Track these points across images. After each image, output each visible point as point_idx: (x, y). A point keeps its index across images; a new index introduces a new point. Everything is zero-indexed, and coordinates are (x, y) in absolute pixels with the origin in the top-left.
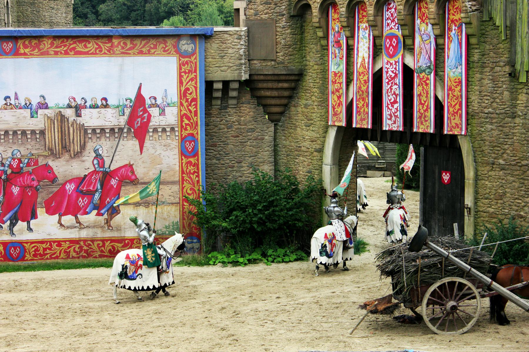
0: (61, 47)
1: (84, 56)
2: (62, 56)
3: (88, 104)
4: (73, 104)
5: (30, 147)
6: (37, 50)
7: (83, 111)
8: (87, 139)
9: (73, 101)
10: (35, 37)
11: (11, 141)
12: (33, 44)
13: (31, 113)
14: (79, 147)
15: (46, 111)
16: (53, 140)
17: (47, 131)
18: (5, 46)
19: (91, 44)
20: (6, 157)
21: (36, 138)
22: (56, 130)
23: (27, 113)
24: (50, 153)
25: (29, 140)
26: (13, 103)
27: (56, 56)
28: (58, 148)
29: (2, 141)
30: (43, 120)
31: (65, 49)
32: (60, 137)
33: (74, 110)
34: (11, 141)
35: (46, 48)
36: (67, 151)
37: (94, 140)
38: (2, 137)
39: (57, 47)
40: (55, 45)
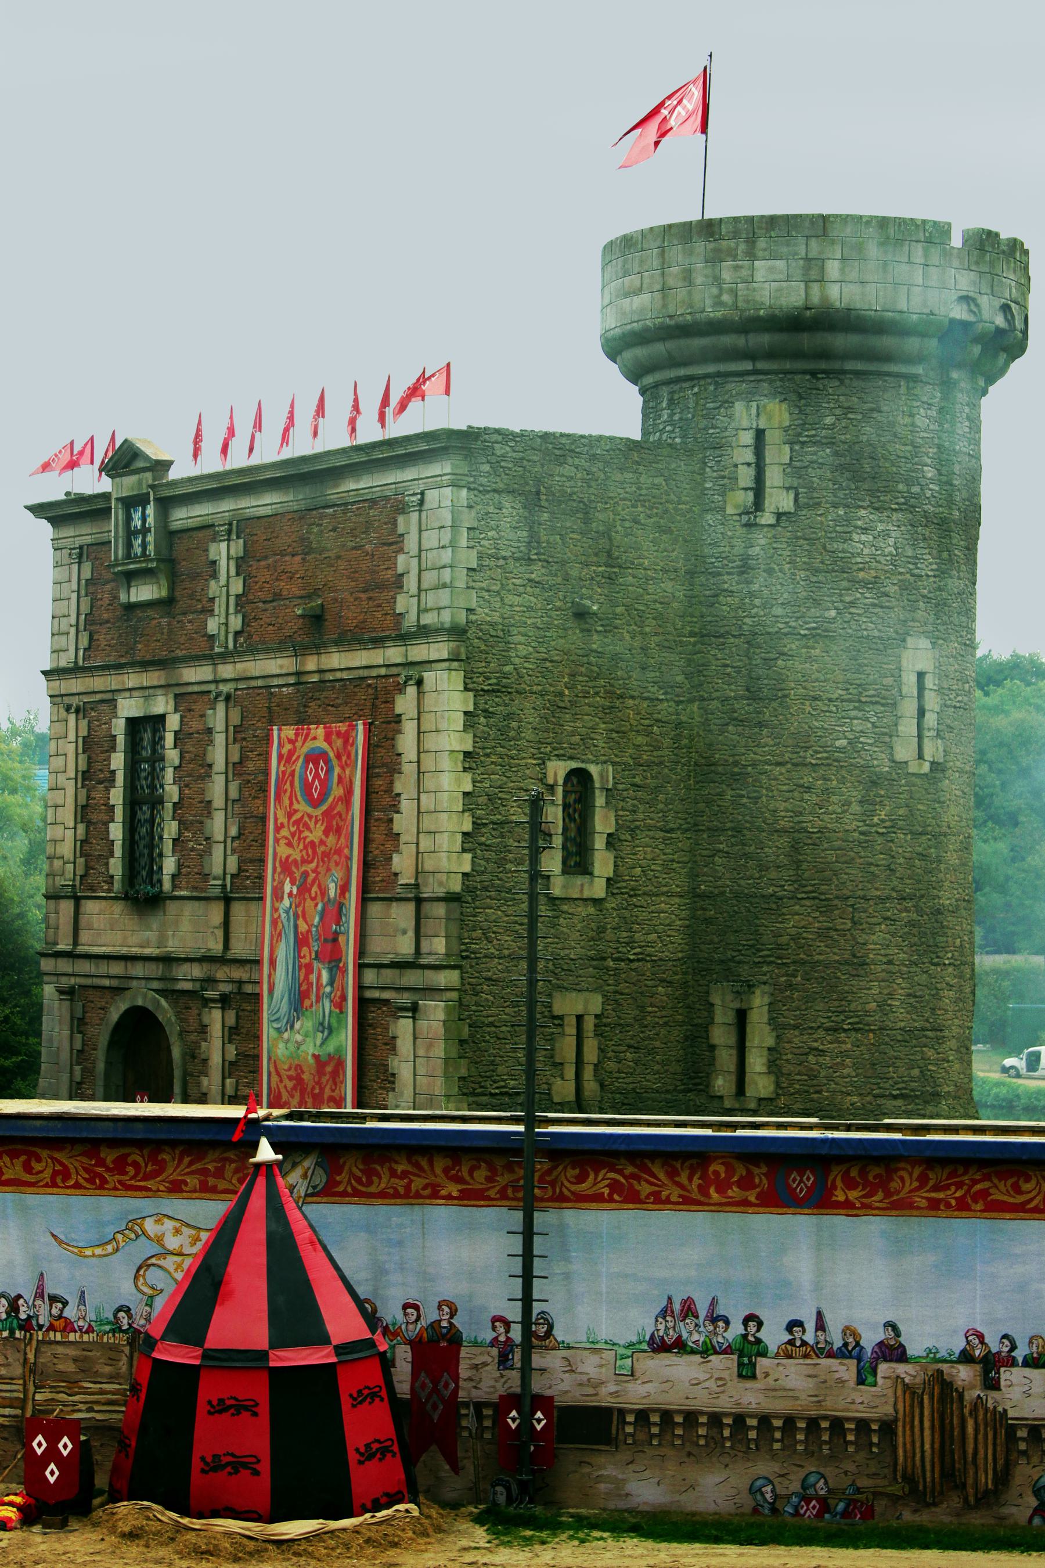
0: (947, 1187)
1: (1012, 1215)
2: (950, 1213)
3: (1019, 1354)
4: (977, 1353)
5: (851, 1467)
6: (880, 1195)
7: (1006, 1375)
8: (1014, 1456)
9: (977, 1341)
10: (877, 1160)
11: (800, 1447)
12: (871, 1178)
13: (859, 1372)
14: (990, 1476)
15: (901, 1369)
16: (918, 1450)
17: (900, 1424)
18: (794, 1180)
19: (1034, 1182)
20: (784, 1492)
21: (871, 1444)
22: (927, 1424)
23: (847, 1370)
24: (907, 1489)
25: (851, 1449)
26: (811, 1342)
27: (933, 1213)
28: (931, 1475)
29: (777, 1446)
30: (890, 1392)
31: (958, 1194)
32: (937, 1446)
33: (978, 1367)
34: (800, 1447)
35: (907, 1189)
36: (956, 1487)
37: (1035, 1460)
38: (778, 1435)
39: (936, 1188)
40: (931, 1183)
